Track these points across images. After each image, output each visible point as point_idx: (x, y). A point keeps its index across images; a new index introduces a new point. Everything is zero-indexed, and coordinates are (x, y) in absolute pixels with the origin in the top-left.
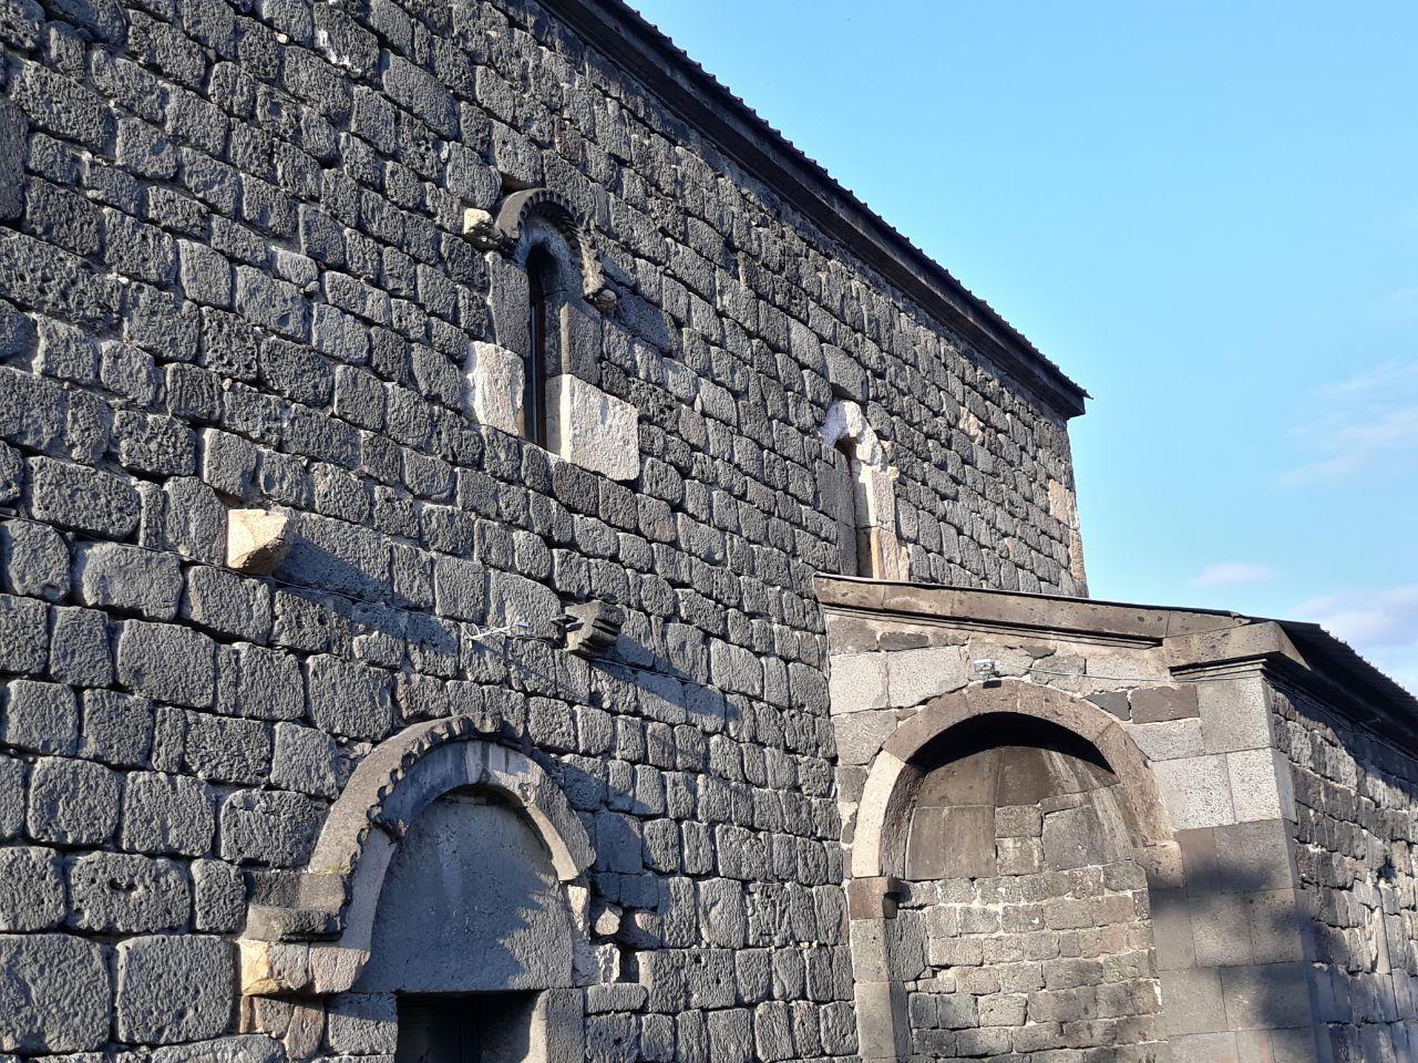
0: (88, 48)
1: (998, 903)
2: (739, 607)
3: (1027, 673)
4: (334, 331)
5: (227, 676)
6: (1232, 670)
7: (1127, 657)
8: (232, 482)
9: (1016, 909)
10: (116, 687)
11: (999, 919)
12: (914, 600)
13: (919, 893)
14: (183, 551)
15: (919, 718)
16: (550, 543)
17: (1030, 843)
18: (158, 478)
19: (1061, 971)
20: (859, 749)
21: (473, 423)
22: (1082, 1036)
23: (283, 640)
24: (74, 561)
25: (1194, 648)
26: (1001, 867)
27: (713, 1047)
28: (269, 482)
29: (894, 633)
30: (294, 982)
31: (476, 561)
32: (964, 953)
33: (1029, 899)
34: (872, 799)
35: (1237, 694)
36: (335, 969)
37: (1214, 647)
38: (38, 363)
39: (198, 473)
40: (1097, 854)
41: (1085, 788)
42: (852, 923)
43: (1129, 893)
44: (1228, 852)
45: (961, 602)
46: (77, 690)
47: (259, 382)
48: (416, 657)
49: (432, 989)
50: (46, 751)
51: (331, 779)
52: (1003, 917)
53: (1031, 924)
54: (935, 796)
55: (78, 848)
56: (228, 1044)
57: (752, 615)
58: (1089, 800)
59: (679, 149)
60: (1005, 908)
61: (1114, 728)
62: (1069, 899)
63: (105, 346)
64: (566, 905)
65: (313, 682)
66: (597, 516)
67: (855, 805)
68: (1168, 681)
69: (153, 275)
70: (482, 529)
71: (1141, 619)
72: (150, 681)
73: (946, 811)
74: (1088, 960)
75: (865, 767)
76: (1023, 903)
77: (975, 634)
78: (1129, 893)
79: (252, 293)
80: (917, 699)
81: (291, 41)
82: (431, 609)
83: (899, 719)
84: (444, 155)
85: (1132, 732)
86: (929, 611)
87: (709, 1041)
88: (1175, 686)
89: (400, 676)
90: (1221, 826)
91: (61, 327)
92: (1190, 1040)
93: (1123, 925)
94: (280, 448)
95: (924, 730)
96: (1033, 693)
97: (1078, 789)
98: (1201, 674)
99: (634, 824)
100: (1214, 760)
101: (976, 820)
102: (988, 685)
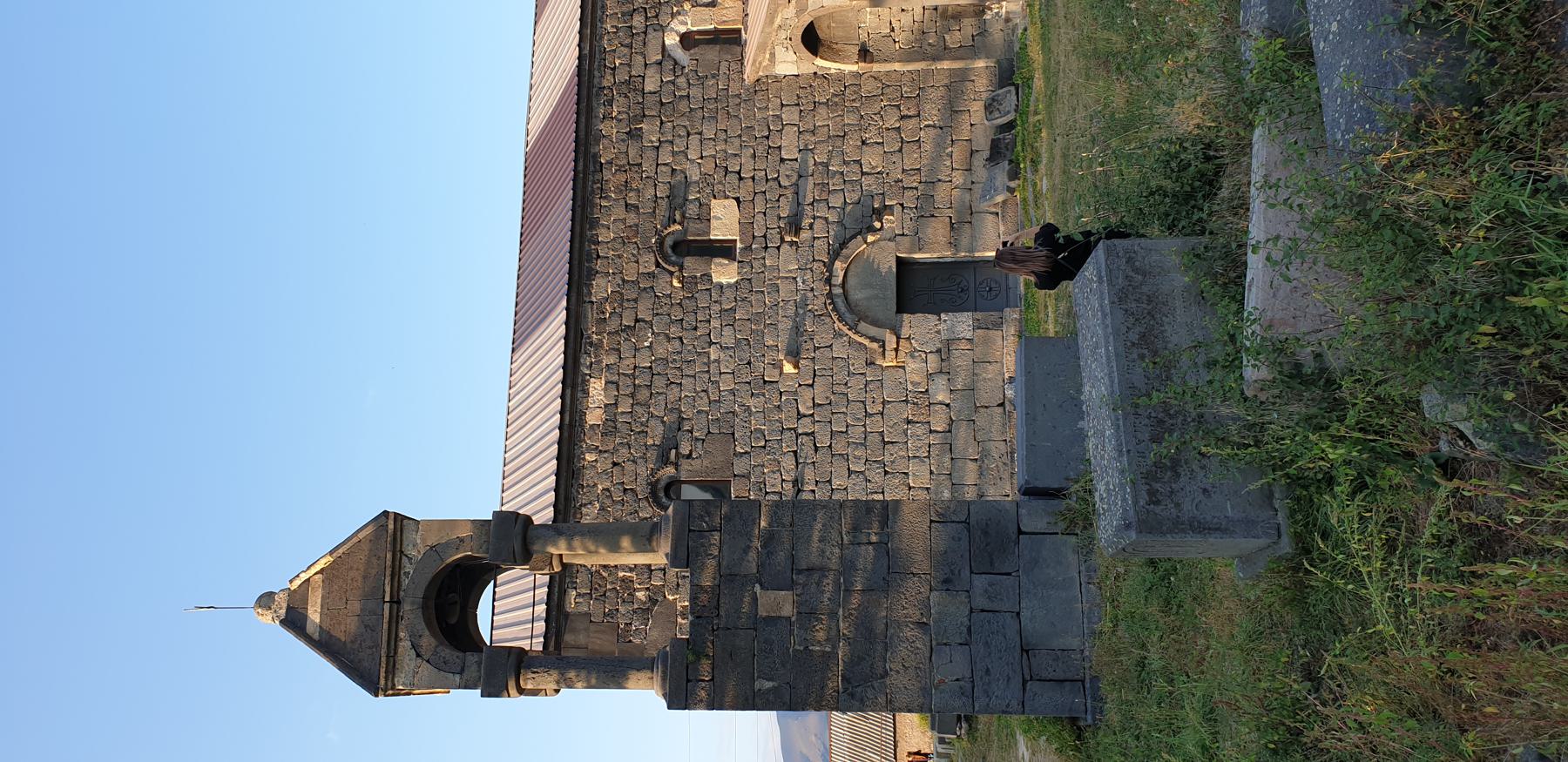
0: (683, 418)
2: (767, 138)
4: (728, 337)
5: (824, 372)
8: (777, 372)
10: (830, 404)
14: (797, 386)
16: (766, 247)
18: (781, 393)
21: (737, 282)
23: (813, 355)
24: (805, 416)
28: (774, 360)
30: (894, 353)
31: (779, 282)
36: (891, 341)
38: (763, 427)
39: (777, 382)
46: (833, 413)
47: (749, 363)
48: (810, 307)
49: (895, 301)
50: (846, 421)
51: (845, 338)
55: (866, 412)
56: (907, 369)
57: (770, 130)
59: (603, 161)
63: (754, 410)
64: (873, 243)
65: (822, 345)
66: (753, 223)
69: (733, 397)
70: (770, 280)
72: (828, 395)
73: (833, 25)
79: (728, 367)
81: (653, 355)
82: (795, 300)
84: (661, 295)
89: (816, 313)
91: (753, 422)
94: (764, 355)
99: (849, 208)
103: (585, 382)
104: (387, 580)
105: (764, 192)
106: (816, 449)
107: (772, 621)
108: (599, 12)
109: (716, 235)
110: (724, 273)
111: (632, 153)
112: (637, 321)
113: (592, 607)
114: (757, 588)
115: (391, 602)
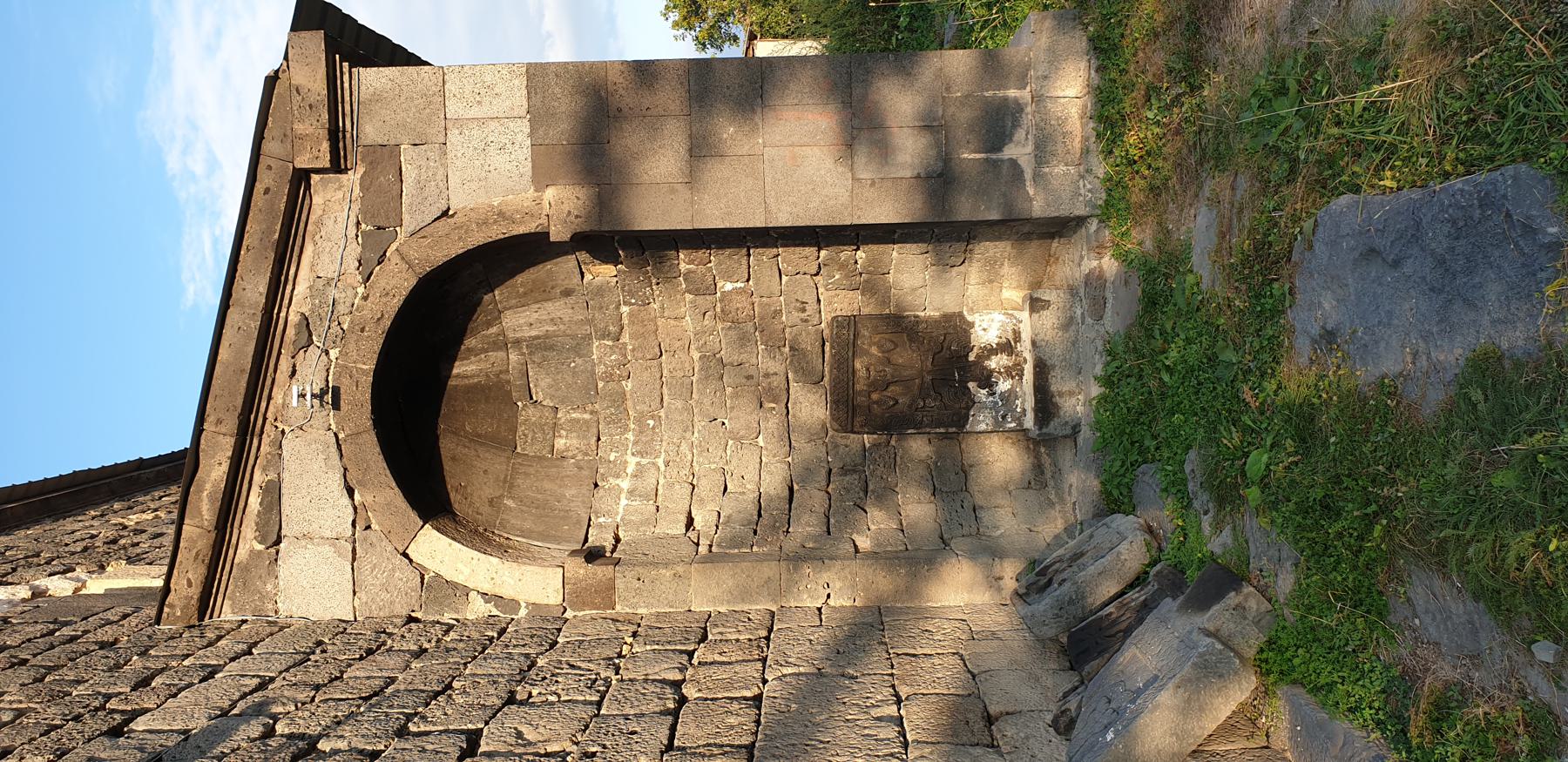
1: (626, 462)
3: (327, 353)
6: (347, 98)
7: (320, 223)
9: (636, 443)
11: (644, 461)
12: (208, 486)
13: (600, 537)
15: (369, 499)
17: (563, 420)
19: (707, 401)
20: (400, 584)
22: (775, 384)
25: (310, 130)
26: (587, 454)
27: (725, 741)
29: (257, 524)
32: (676, 501)
33: (626, 429)
34: (467, 571)
35: (377, 98)
37: (311, 106)
40: (580, 346)
41: (502, 344)
42: (618, 608)
43: (625, 309)
44: (562, 130)
45: (219, 422)
52: (642, 457)
53: (653, 428)
54: (486, 509)
58: (517, 342)
60: (633, 454)
61: (404, 250)
62: (629, 385)
67: (473, 595)
68: (353, 178)
71: (267, 191)
73: (510, 503)
74: (696, 370)
75: (426, 577)
76: (630, 436)
77: (270, 415)
78: (625, 309)
80: (346, 500)
83: (368, 527)
85: (411, 229)
86: (225, 467)
87: (715, 745)
88: (361, 170)
90: (531, 135)
92: (771, 201)
93: (659, 323)
95: (385, 494)
96: (352, 346)
97: (502, 354)
98: (348, 135)
100: (454, 137)
101: (527, 474)
102: (336, 405)
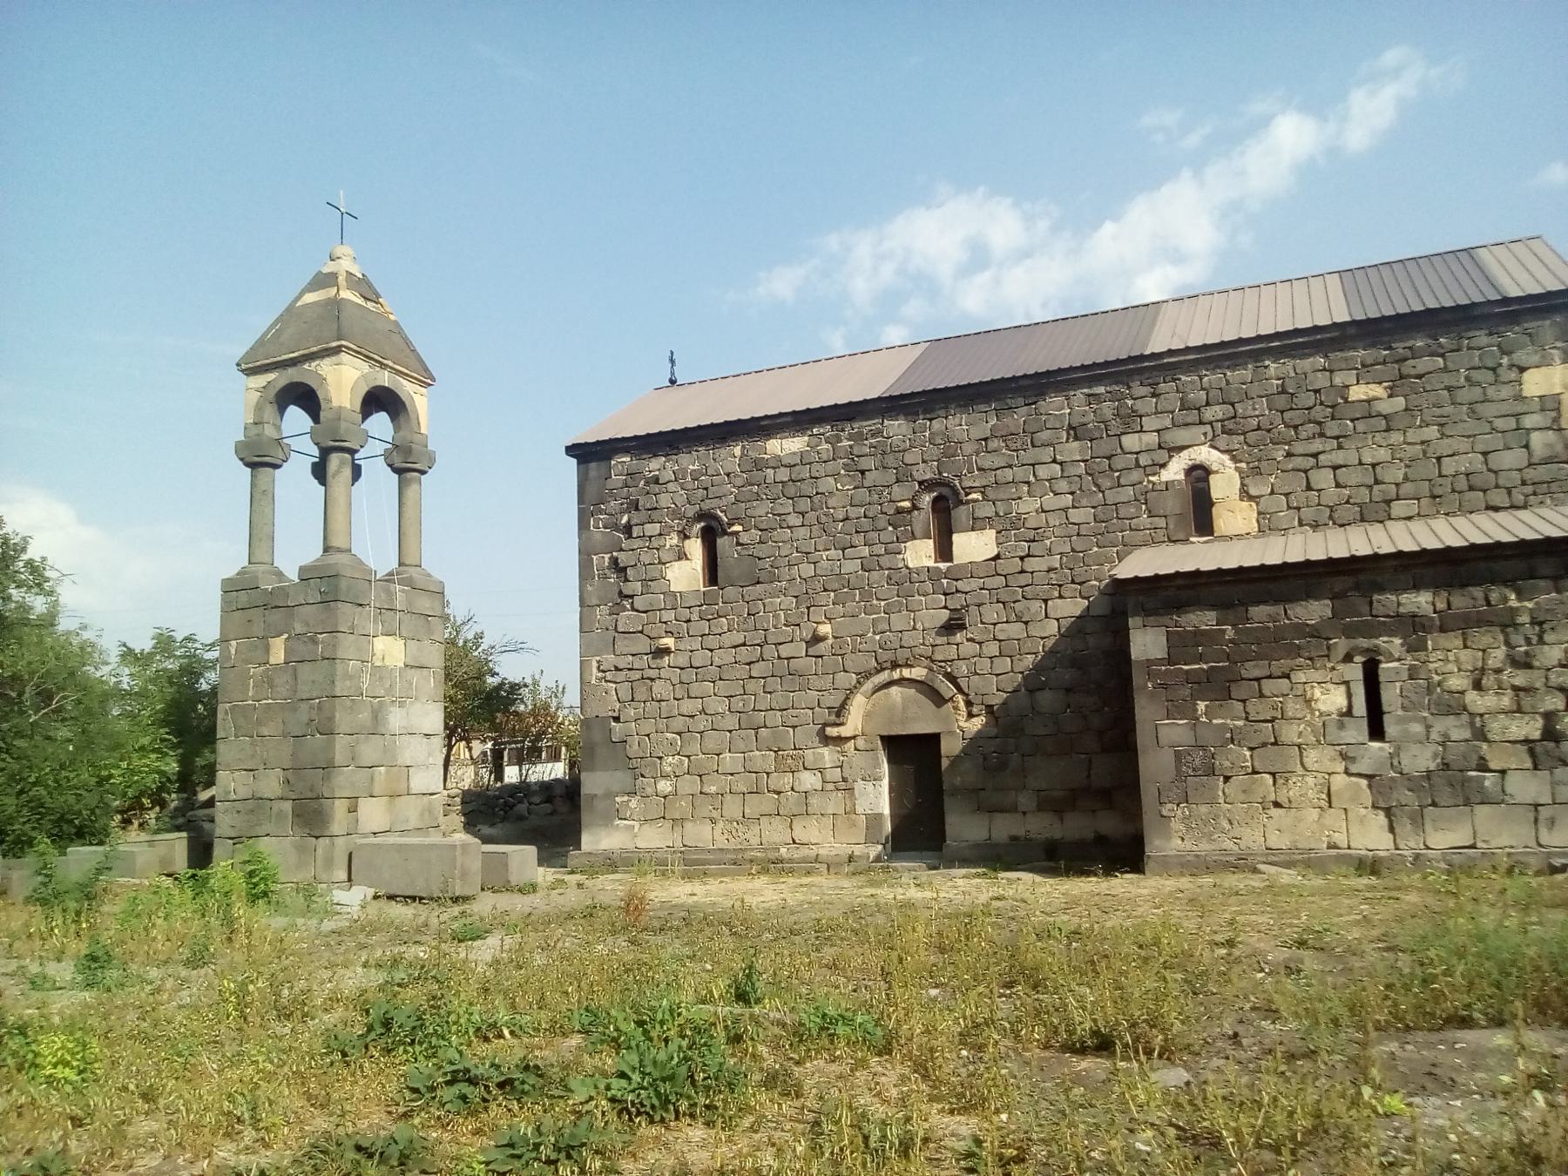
66: (972, 577)
103: (803, 434)
104: (302, 352)
105: (1007, 586)
106: (749, 664)
107: (267, 649)
108: (1227, 363)
109: (957, 538)
110: (920, 553)
111: (1044, 436)
112: (863, 472)
113: (617, 479)
114: (286, 636)
115: (291, 359)
